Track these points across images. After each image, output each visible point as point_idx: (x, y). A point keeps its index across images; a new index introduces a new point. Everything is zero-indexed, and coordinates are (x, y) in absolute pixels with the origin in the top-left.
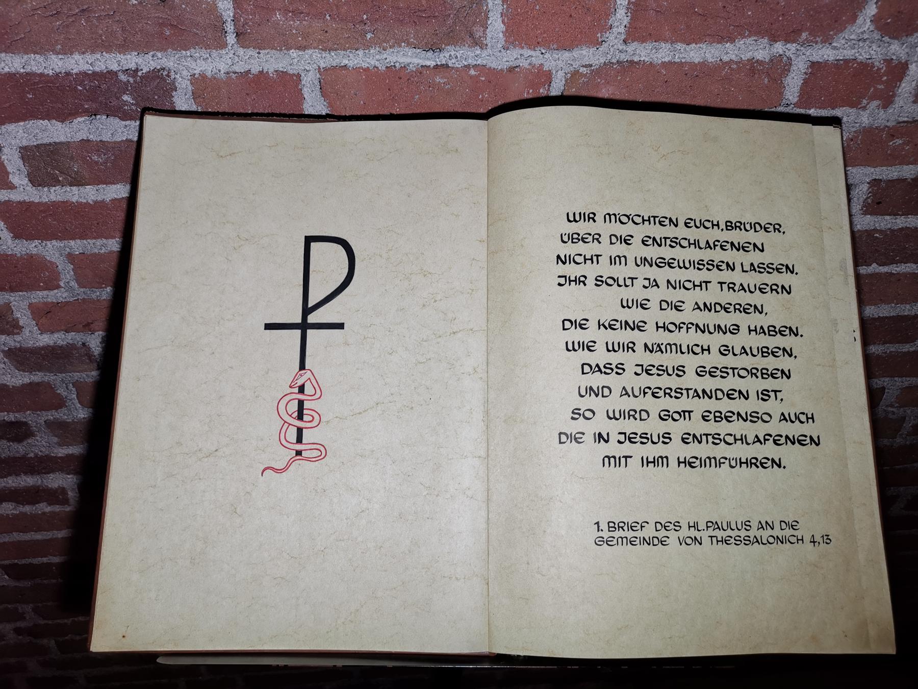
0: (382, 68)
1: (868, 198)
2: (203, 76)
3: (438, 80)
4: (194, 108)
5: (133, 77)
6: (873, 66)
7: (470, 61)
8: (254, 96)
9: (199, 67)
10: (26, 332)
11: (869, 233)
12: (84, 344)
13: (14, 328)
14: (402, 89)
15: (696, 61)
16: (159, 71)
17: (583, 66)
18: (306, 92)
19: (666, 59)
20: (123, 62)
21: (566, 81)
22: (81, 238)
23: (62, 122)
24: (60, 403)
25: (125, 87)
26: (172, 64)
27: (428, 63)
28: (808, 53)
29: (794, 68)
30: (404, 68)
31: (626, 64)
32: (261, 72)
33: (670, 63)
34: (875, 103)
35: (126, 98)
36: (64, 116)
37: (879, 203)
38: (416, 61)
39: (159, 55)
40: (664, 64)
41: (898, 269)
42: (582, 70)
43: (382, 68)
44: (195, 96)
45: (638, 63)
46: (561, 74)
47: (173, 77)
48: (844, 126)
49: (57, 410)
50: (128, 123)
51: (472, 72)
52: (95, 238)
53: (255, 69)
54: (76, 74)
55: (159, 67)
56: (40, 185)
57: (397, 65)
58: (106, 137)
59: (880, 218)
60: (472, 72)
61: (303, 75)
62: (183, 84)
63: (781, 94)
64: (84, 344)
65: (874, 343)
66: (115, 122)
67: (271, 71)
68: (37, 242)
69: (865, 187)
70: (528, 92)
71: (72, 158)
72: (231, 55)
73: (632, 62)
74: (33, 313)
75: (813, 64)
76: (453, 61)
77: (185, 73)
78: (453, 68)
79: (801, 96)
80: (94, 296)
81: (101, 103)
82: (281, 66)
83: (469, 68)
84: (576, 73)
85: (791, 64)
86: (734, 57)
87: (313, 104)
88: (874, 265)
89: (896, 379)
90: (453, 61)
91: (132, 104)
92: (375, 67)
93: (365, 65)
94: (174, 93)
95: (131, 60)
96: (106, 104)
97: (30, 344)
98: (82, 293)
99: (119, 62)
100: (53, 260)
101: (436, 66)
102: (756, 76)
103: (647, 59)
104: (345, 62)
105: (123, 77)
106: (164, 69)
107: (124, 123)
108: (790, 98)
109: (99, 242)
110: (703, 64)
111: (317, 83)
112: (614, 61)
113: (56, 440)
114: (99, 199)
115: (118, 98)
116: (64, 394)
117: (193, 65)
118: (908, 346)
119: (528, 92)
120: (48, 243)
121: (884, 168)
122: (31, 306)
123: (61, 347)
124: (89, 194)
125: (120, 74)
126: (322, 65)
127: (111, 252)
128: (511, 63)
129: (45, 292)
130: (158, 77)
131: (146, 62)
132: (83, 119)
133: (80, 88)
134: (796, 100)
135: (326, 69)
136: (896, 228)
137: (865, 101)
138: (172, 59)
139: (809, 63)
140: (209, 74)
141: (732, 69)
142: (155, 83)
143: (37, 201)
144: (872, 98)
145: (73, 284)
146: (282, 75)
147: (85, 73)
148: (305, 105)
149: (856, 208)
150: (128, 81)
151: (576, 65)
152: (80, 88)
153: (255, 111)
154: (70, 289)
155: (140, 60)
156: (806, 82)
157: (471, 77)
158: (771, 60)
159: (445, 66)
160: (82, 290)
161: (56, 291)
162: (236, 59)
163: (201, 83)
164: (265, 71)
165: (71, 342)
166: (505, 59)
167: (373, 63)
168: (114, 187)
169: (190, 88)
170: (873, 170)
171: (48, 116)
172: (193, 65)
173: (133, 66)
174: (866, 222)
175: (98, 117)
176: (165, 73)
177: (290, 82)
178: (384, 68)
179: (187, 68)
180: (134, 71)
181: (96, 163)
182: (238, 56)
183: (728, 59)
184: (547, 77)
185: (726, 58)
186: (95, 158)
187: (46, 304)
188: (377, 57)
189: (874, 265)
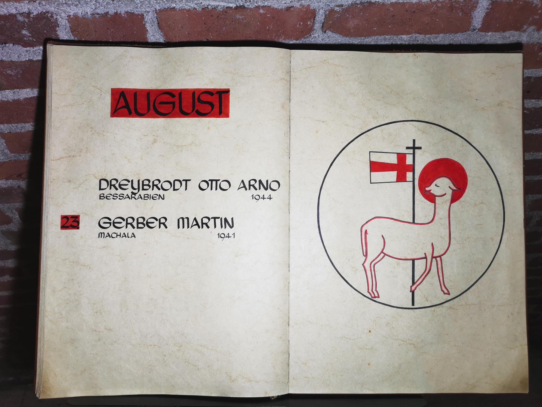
0: (199, 9)
2: (76, 17)
3: (238, 16)
4: (72, 38)
5: (27, 18)
7: (260, 3)
8: (112, 30)
9: (72, 11)
12: (19, 187)
14: (214, 23)
17: (337, 6)
18: (148, 26)
20: (19, 8)
21: (325, 16)
22: (7, 123)
24: (8, 221)
25: (22, 25)
26: (53, 9)
27: (231, 5)
29: (480, 5)
30: (215, 8)
32: (116, 13)
34: (532, 28)
35: (24, 32)
38: (222, 4)
39: (44, 3)
41: (537, 132)
42: (337, 9)
43: (199, 9)
45: (373, 3)
46: (321, 12)
47: (55, 17)
49: (7, 225)
50: (28, 49)
51: (261, 11)
52: (17, 123)
53: (112, 11)
55: (44, 11)
57: (210, 7)
58: (15, 58)
60: (261, 11)
61: (145, 15)
62: (63, 22)
63: (470, 23)
64: (19, 187)
66: (19, 49)
67: (123, 12)
70: (300, 24)
72: (94, 2)
73: (370, 3)
76: (248, 4)
77: (63, 15)
78: (248, 8)
80: (21, 158)
82: (129, 9)
83: (259, 9)
84: (332, 11)
85: (478, 3)
87: (154, 34)
89: (529, 195)
90: (248, 4)
91: (29, 36)
92: (195, 9)
93: (187, 7)
94: (57, 29)
95: (25, 7)
98: (12, 156)
99: (16, 8)
101: (237, 8)
102: (454, 11)
104: (174, 5)
105: (20, 18)
106: (48, 12)
107: (25, 49)
108: (476, 25)
109: (20, 125)
110: (418, 4)
111: (155, 20)
112: (358, 2)
113: (9, 241)
114: (16, 98)
115: (19, 32)
116: (11, 215)
117: (68, 9)
118: (538, 177)
119: (300, 24)
121: (534, 70)
123: (5, 189)
124: (8, 95)
125: (18, 16)
126: (158, 8)
127: (28, 132)
128: (288, 5)
130: (45, 18)
131: (36, 9)
134: (479, 26)
136: (538, 107)
137: (525, 27)
138: (53, 5)
140: (80, 15)
144: (530, 25)
145: (6, 151)
146: (131, 15)
148: (148, 35)
150: (24, 21)
151: (332, 5)
153: (115, 40)
154: (5, 154)
155: (31, 7)
156: (487, 14)
157: (261, 14)
159: (242, 7)
160: (13, 154)
162: (98, 5)
163: (75, 22)
164: (119, 12)
165: (10, 185)
166: (283, 2)
167: (192, 6)
168: (25, 91)
169: (68, 25)
172: (68, 9)
173: (26, 10)
175: (7, 45)
177: (136, 20)
178: (200, 10)
179: (65, 12)
181: (11, 75)
182: (99, 3)
184: (313, 14)
186: (9, 72)
188: (195, 2)
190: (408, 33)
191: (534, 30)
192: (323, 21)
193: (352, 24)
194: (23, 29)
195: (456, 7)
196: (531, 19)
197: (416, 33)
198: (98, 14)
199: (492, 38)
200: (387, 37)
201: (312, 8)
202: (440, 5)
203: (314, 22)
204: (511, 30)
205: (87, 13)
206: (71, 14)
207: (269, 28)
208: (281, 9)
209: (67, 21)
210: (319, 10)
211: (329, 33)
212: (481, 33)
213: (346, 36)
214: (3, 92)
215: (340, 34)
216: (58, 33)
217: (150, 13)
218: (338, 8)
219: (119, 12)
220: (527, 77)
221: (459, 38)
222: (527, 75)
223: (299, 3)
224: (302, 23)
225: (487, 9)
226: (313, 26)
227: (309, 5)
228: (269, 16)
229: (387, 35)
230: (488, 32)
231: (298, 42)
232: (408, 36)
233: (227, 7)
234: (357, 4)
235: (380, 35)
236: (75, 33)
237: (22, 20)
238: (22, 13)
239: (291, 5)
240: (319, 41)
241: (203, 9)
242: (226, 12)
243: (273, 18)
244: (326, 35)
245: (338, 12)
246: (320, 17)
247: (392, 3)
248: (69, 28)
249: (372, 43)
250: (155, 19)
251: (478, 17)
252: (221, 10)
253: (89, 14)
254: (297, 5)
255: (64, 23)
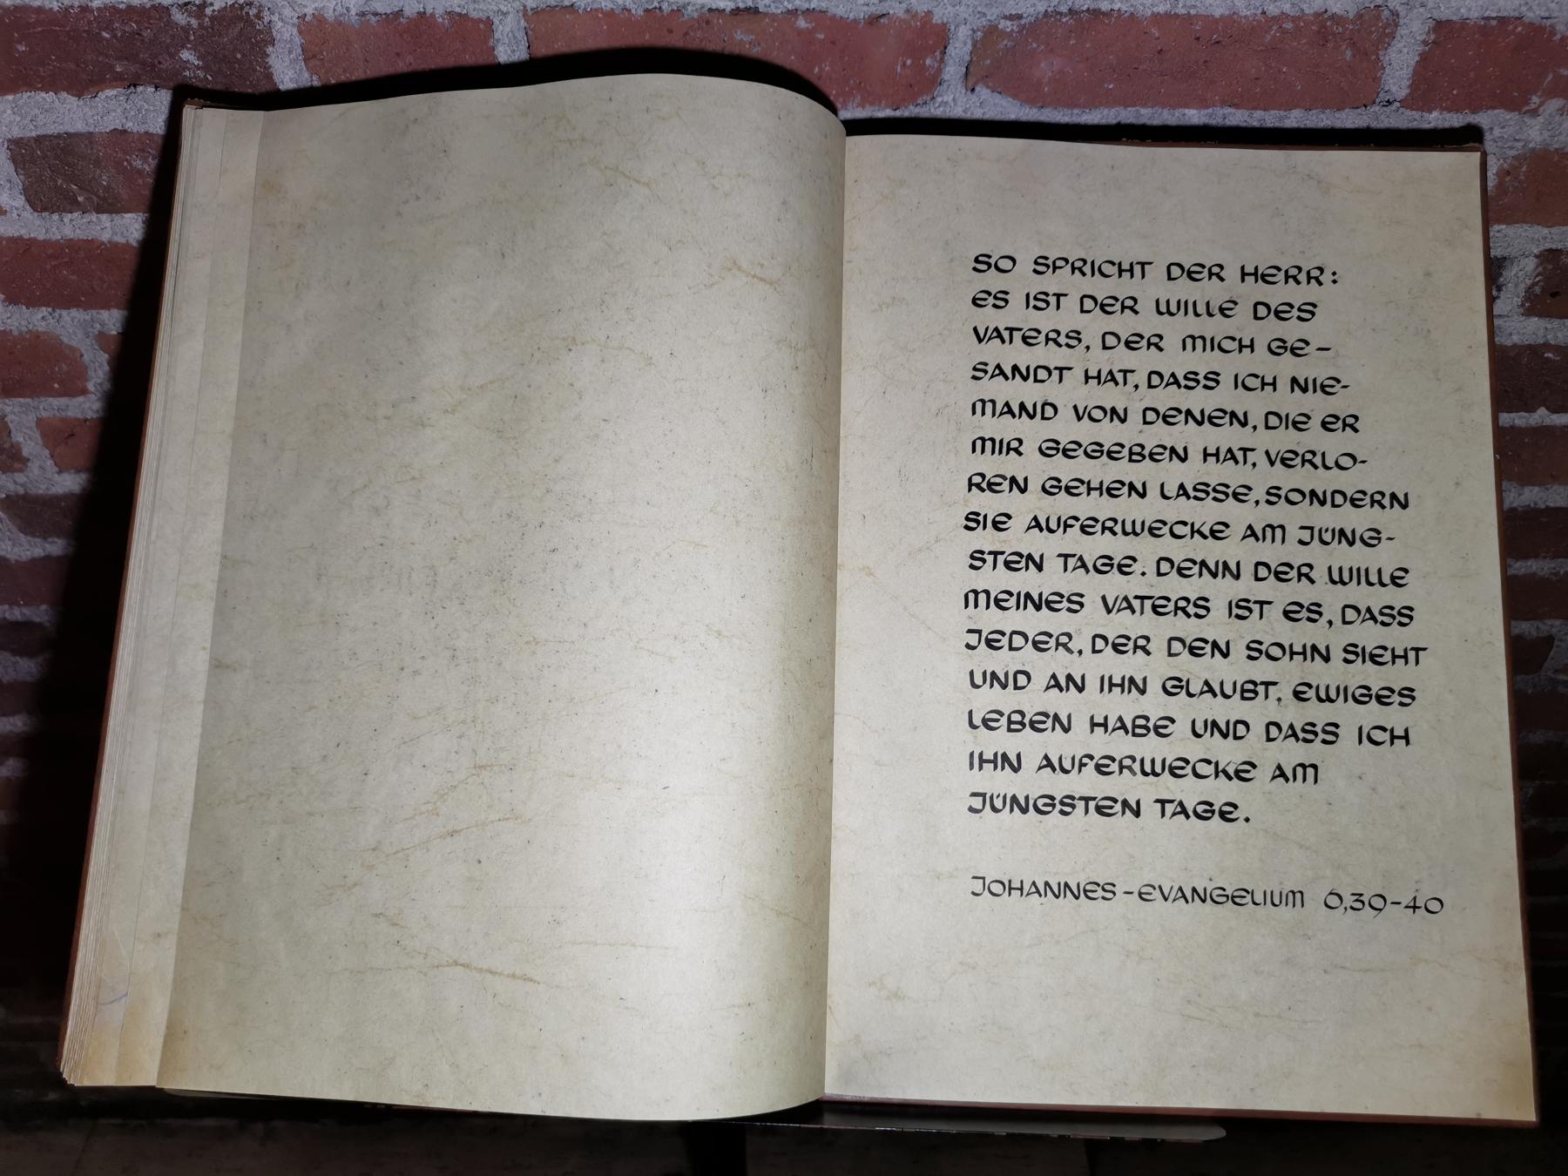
1: (1534, 284)
2: (319, 19)
6: (1553, 32)
7: (797, 3)
10: (34, 469)
11: (1535, 350)
13: (12, 459)
15: (1217, 13)
16: (242, 7)
17: (1005, 17)
19: (1161, 9)
21: (974, 45)
23: (79, 96)
25: (183, 37)
28: (1430, 5)
29: (1402, 31)
31: (1085, 16)
32: (422, 15)
33: (1167, 15)
34: (1555, 104)
35: (186, 55)
36: (83, 84)
37: (1554, 295)
40: (1157, 18)
42: (1006, 25)
44: (309, 56)
45: (1104, 14)
47: (266, 20)
48: (1489, 145)
54: (99, 9)
56: (45, 210)
57: (665, 6)
59: (1556, 323)
60: (802, 23)
61: (496, 21)
62: (285, 31)
63: (1377, 80)
65: (1536, 556)
67: (439, 11)
68: (44, 311)
69: (1530, 264)
71: (97, 163)
73: (1096, 13)
74: (44, 435)
75: (1440, 26)
77: (287, 12)
78: (766, 14)
79: (1414, 86)
81: (144, 63)
84: (991, 31)
85: (1397, 25)
86: (1287, 8)
88: (1542, 411)
91: (198, 67)
92: (625, 9)
94: (270, 49)
96: (153, 66)
97: (41, 489)
100: (74, 344)
101: (737, 11)
103: (1124, 8)
105: (179, 18)
106: (250, 4)
108: (1394, 89)
110: (1230, 20)
111: (521, 35)
112: (1064, 9)
115: (172, 56)
119: (904, 64)
120: (64, 312)
122: (40, 423)
125: (174, 11)
128: (872, 9)
129: (64, 401)
130: (241, 18)
132: (114, 92)
133: (105, 35)
134: (1404, 93)
135: (536, 11)
139: (1431, 23)
140: (329, 15)
141: (1284, 32)
142: (237, 30)
143: (41, 237)
144: (1551, 93)
147: (114, 7)
149: (1509, 302)
150: (189, 24)
151: (993, 14)
152: (105, 35)
156: (1424, 59)
157: (800, 32)
158: (1359, 16)
159: (753, 11)
161: (81, 399)
163: (315, 30)
164: (429, 11)
169: (298, 40)
170: (1546, 231)
171: (51, 85)
174: (1526, 330)
175: (140, 89)
176: (253, 12)
178: (641, 12)
180: (198, 6)
181: (140, 172)
183: (1276, 12)
185: (1273, 10)
186: (138, 163)
187: (64, 420)
189: (1542, 411)
190: (1203, 104)
191: (1561, 111)
192: (967, 58)
193: (1046, 68)
194: (183, 47)
195: (1334, 34)
196: (1550, 77)
197: (1224, 103)
198: (376, 14)
199: (1435, 119)
200: (1143, 111)
201: (936, 19)
202: (1289, 26)
203: (942, 60)
204: (1493, 108)
205: (348, 9)
206: (309, 11)
207: (821, 70)
208: (855, 20)
209: (295, 31)
210: (957, 26)
211: (983, 92)
212: (1408, 112)
213: (1030, 101)
214: (116, 217)
215: (1015, 96)
216: (272, 60)
217: (509, 18)
218: (1009, 23)
219: (429, 11)
220: (1550, 251)
221: (1349, 119)
222: (1548, 246)
223: (904, 5)
224: (909, 62)
225: (1425, 42)
226: (940, 71)
227: (929, 13)
228: (822, 36)
229: (1144, 105)
230: (1430, 112)
231: (898, 114)
232: (1204, 112)
233: (710, 10)
234: (1061, 14)
235: (1126, 107)
236: (312, 63)
237: (183, 23)
238: (186, 4)
239: (880, 9)
240: (957, 112)
241: (647, 11)
242: (708, 22)
243: (833, 43)
244: (974, 98)
245: (1010, 35)
246: (960, 48)
247: (1156, 16)
248: (299, 51)
249: (1104, 122)
250: (522, 33)
251: (1399, 65)
252: (695, 15)
253: (353, 12)
254: (897, 10)
255: (287, 36)
